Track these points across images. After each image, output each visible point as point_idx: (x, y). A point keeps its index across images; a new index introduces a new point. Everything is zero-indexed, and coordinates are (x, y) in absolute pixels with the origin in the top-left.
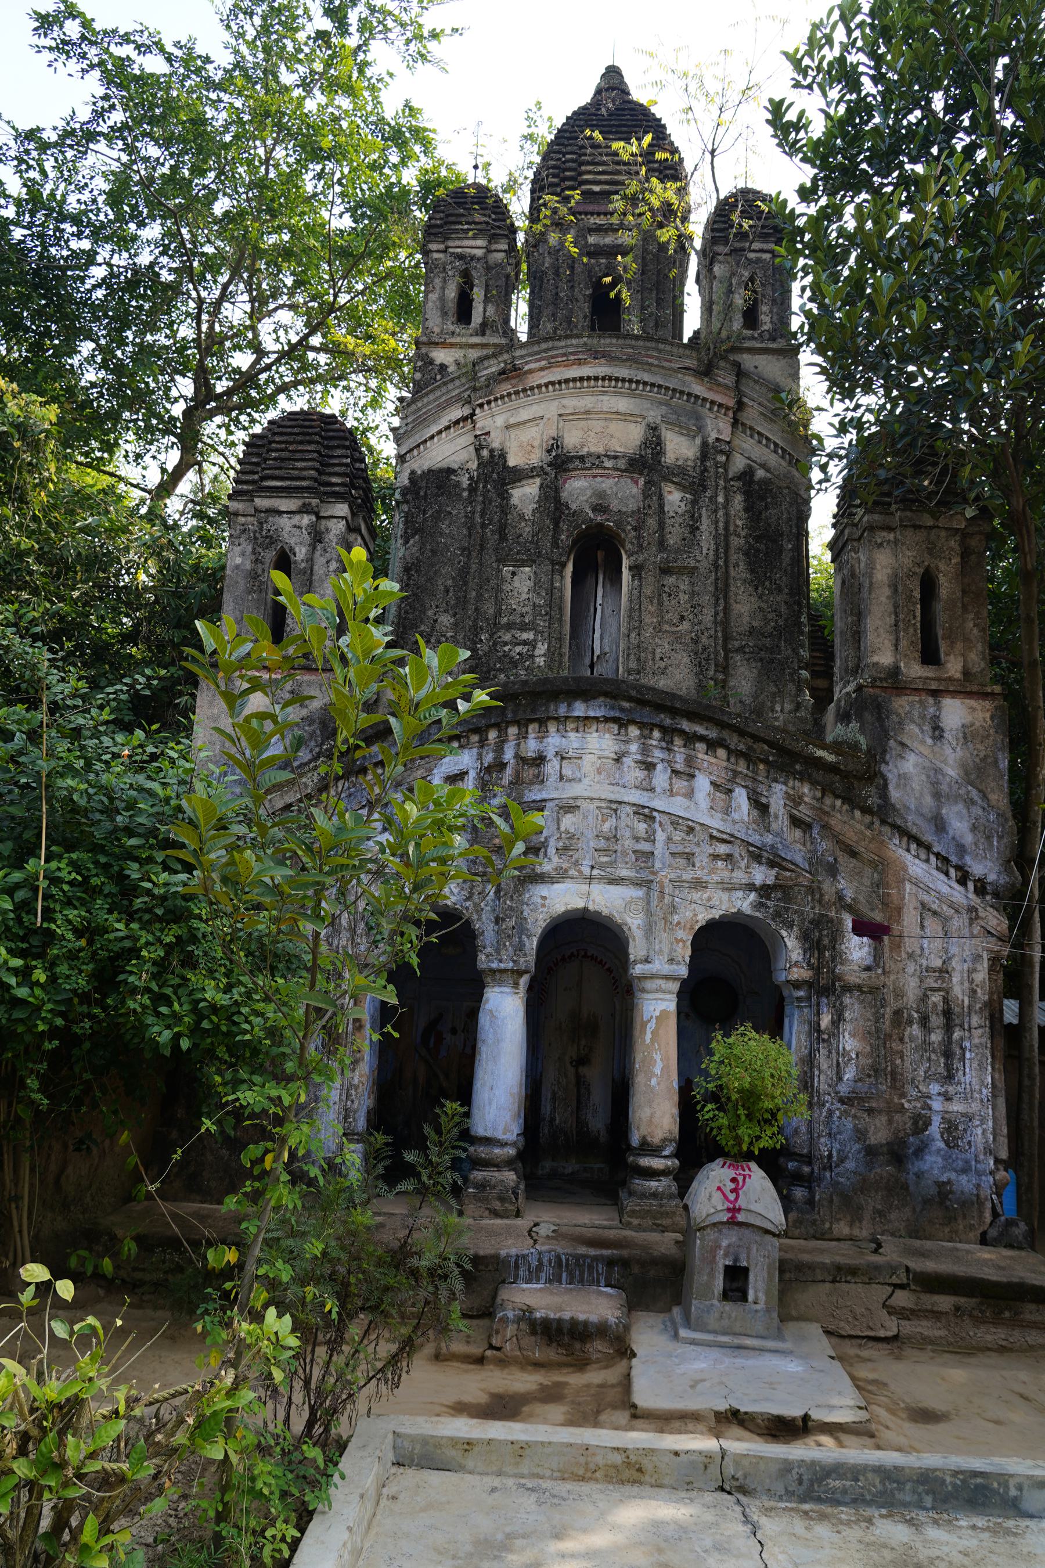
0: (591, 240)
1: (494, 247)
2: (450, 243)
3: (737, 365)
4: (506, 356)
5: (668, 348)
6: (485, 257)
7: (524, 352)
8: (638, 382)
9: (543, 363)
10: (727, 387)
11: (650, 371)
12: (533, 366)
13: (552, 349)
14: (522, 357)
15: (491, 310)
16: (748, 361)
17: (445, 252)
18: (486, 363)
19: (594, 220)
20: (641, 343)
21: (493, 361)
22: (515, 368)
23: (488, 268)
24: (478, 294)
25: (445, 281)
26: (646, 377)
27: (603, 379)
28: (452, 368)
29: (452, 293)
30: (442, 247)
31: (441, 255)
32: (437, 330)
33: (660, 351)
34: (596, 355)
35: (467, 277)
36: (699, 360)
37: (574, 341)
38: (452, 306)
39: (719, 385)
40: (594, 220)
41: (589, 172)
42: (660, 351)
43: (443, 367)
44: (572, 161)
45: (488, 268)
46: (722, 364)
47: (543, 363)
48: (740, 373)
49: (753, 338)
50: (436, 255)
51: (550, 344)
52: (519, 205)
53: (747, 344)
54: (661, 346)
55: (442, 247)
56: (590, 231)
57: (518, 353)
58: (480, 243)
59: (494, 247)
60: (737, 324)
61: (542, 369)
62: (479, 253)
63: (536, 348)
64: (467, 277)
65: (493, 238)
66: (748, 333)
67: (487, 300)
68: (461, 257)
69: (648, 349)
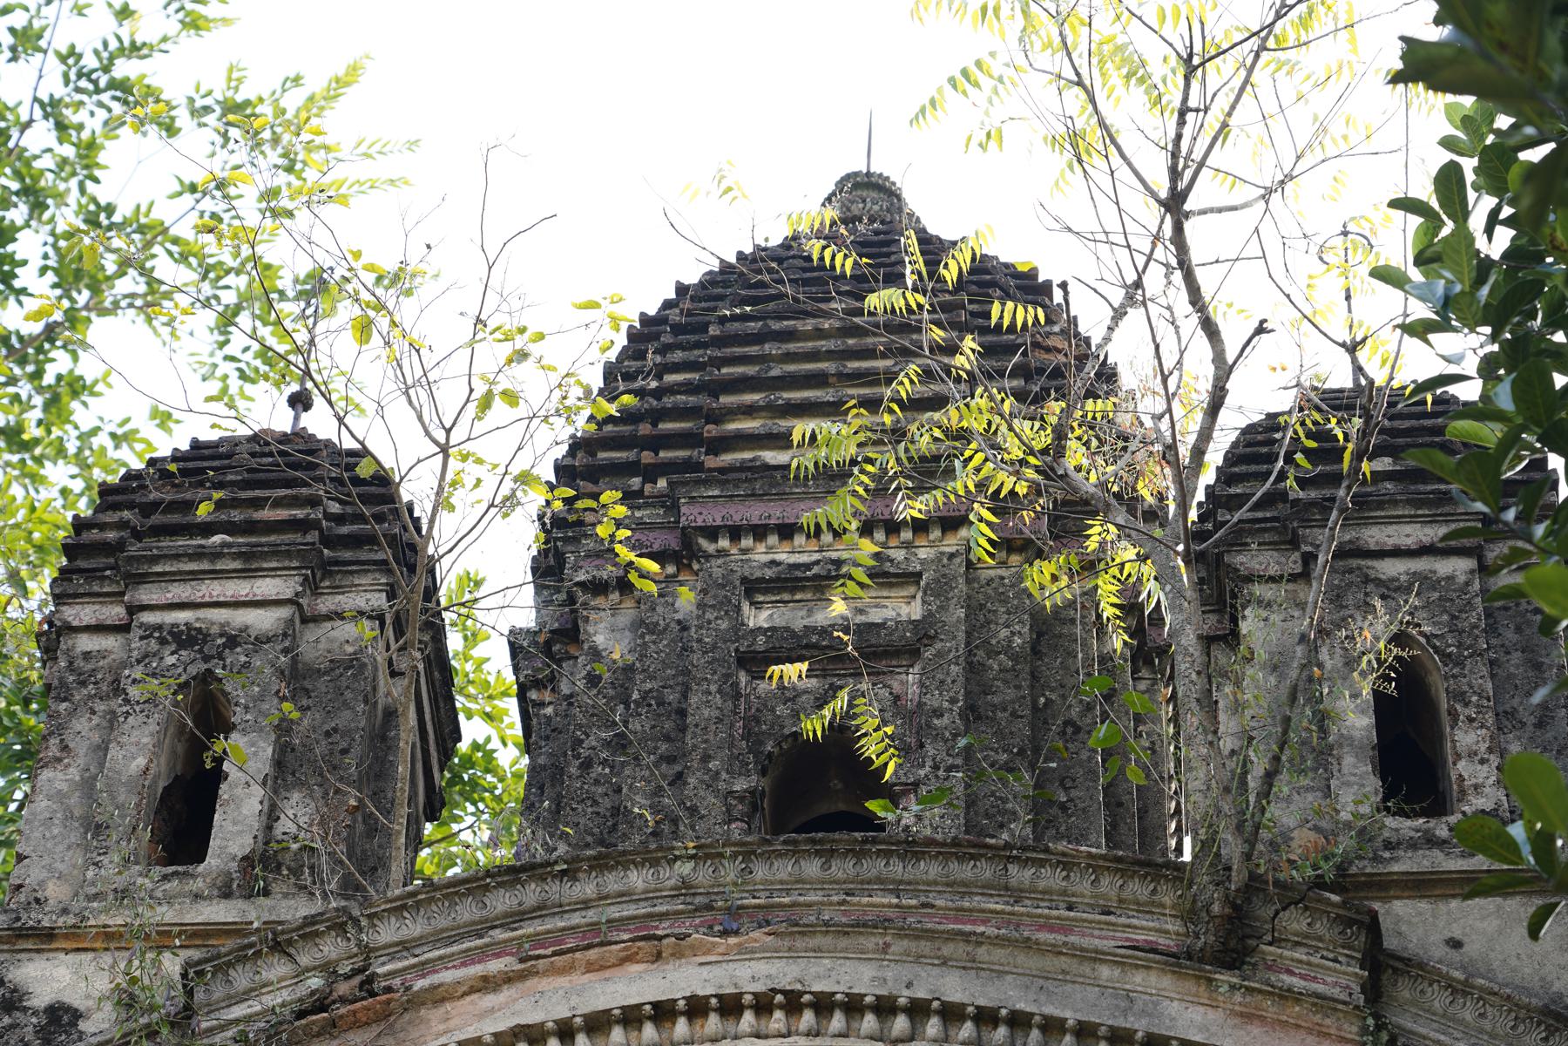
0: (758, 618)
1: (326, 604)
2: (148, 594)
3: (1373, 927)
4: (331, 948)
5: (1051, 878)
6: (288, 636)
7: (413, 927)
8: (918, 1010)
9: (495, 966)
10: (1323, 1003)
11: (971, 965)
12: (447, 976)
13: (540, 910)
14: (405, 946)
15: (297, 814)
16: (1411, 923)
17: (122, 629)
18: (241, 978)
19: (763, 554)
20: (930, 869)
21: (277, 969)
22: (368, 986)
23: (298, 678)
24: (246, 756)
25: (112, 719)
26: (955, 988)
27: (763, 1006)
28: (100, 1021)
29: (138, 753)
30: (114, 613)
31: (110, 642)
32: (55, 892)
33: (1017, 894)
34: (729, 920)
35: (207, 713)
36: (1189, 915)
37: (637, 879)
38: (127, 807)
39: (1287, 995)
40: (763, 554)
41: (750, 411)
42: (1017, 894)
43: (61, 1017)
44: (689, 389)
45: (298, 678)
46: (1295, 922)
47: (495, 966)
48: (1383, 967)
49: (1431, 841)
50: (86, 643)
51: (531, 894)
52: (490, 570)
53: (1406, 864)
54: (1020, 875)
55: (114, 613)
56: (754, 588)
57: (387, 933)
58: (267, 587)
59: (326, 604)
60: (1357, 786)
61: (487, 984)
62: (263, 620)
63: (467, 911)
64: (207, 713)
65: (322, 572)
66: (1407, 826)
67: (285, 771)
68: (187, 638)
69: (964, 888)
